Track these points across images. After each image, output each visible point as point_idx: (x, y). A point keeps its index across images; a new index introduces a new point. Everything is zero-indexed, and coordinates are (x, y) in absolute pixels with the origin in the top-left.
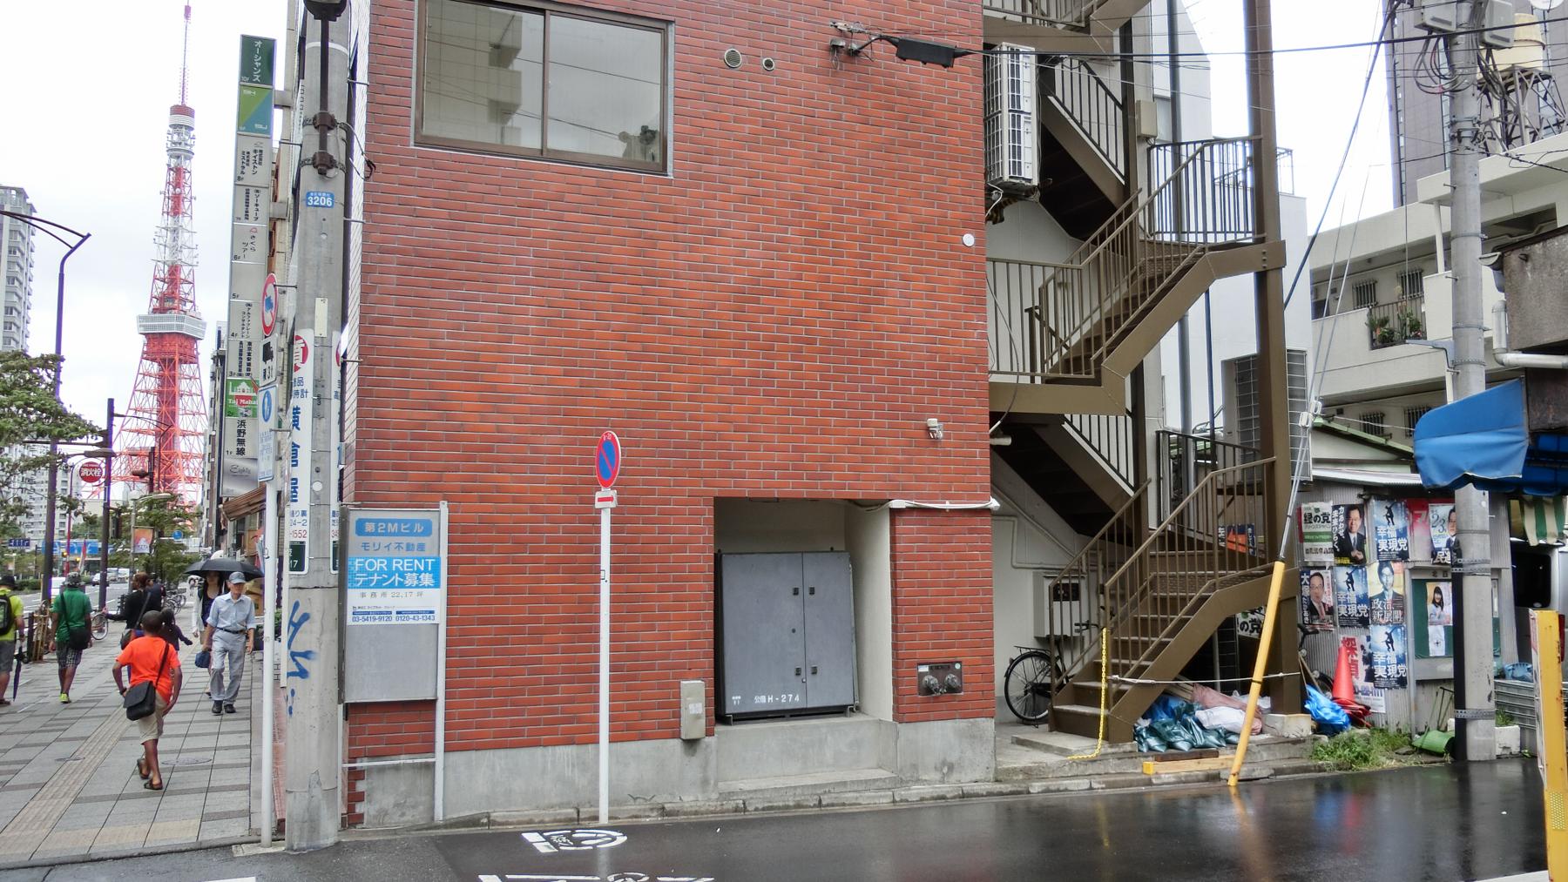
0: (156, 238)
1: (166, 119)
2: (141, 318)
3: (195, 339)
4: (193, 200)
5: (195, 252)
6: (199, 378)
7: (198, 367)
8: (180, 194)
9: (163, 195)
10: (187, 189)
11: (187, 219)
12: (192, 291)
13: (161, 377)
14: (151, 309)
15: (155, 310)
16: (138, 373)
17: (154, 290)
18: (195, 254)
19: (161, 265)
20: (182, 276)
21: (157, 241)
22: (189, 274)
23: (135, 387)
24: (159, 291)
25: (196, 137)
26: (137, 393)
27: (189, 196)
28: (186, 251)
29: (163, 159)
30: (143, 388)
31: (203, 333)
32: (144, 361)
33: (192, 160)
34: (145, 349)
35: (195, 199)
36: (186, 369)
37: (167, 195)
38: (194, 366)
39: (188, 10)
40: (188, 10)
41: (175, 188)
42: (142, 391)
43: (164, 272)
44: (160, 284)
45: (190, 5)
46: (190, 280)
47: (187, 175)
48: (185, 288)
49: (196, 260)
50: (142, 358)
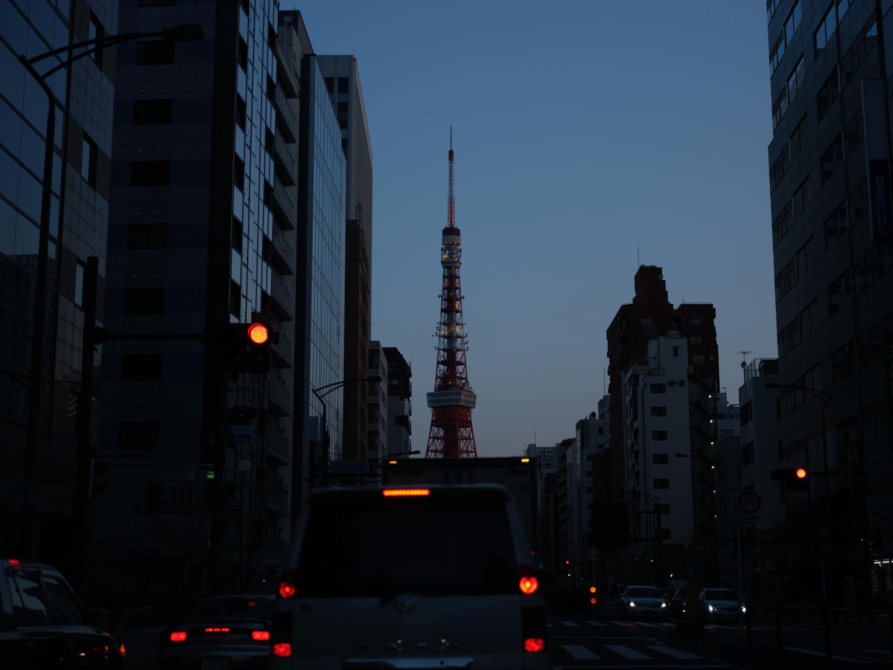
0: (438, 332)
1: (437, 241)
2: (429, 395)
3: (469, 409)
4: (462, 299)
5: (466, 340)
6: (473, 439)
7: (472, 430)
8: (453, 296)
9: (441, 298)
10: (458, 291)
11: (458, 315)
12: (465, 370)
13: (444, 439)
14: (436, 388)
15: (439, 388)
16: (430, 438)
17: (438, 372)
18: (465, 341)
19: (442, 352)
20: (458, 360)
21: (438, 334)
22: (462, 358)
23: (428, 448)
24: (441, 372)
25: (462, 250)
26: (430, 453)
27: (459, 296)
28: (459, 340)
29: (440, 271)
30: (434, 448)
31: (474, 403)
32: (433, 428)
33: (460, 269)
34: (434, 419)
35: (463, 297)
36: (464, 432)
37: (444, 298)
38: (469, 429)
39: (451, 153)
40: (451, 153)
41: (449, 292)
42: (432, 451)
43: (444, 355)
44: (442, 367)
45: (453, 149)
46: (463, 361)
47: (457, 280)
48: (460, 368)
49: (466, 346)
50: (432, 425)
